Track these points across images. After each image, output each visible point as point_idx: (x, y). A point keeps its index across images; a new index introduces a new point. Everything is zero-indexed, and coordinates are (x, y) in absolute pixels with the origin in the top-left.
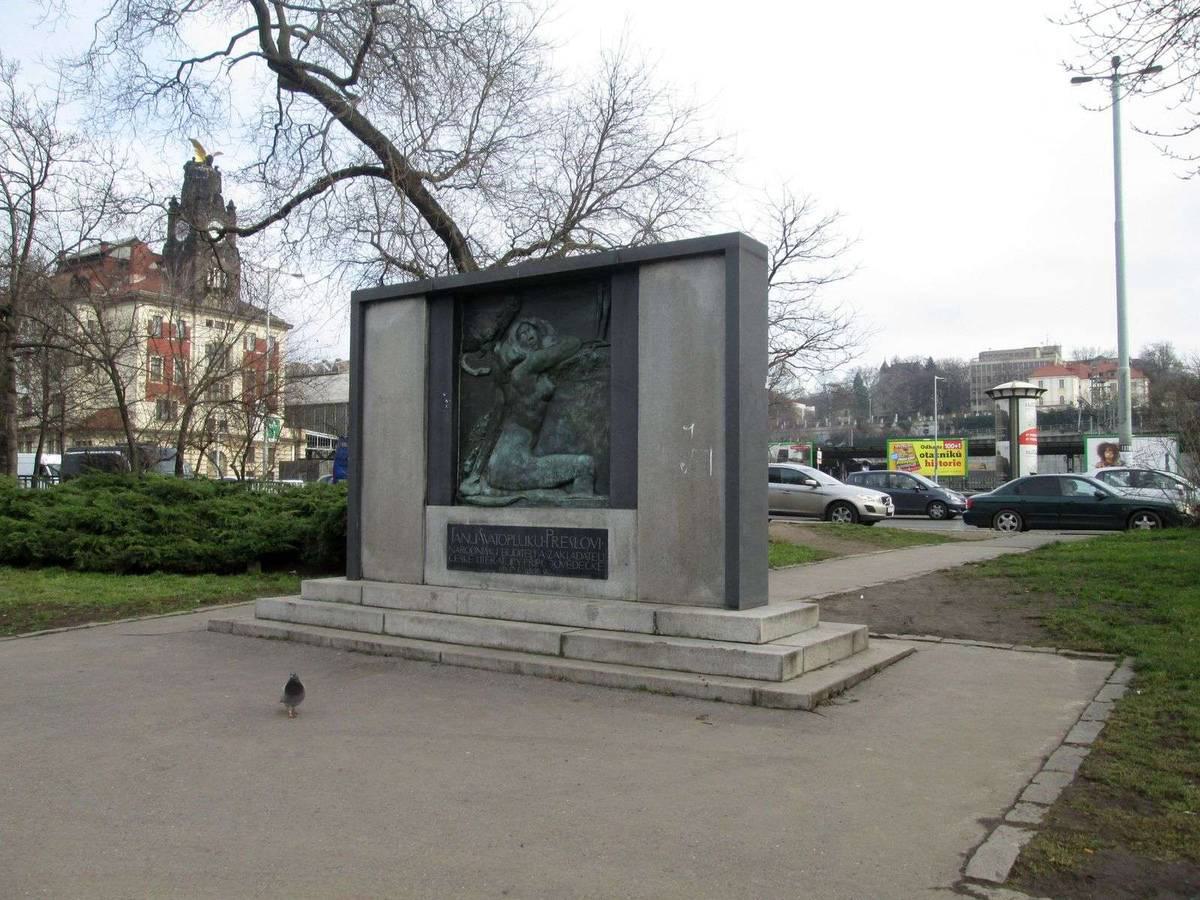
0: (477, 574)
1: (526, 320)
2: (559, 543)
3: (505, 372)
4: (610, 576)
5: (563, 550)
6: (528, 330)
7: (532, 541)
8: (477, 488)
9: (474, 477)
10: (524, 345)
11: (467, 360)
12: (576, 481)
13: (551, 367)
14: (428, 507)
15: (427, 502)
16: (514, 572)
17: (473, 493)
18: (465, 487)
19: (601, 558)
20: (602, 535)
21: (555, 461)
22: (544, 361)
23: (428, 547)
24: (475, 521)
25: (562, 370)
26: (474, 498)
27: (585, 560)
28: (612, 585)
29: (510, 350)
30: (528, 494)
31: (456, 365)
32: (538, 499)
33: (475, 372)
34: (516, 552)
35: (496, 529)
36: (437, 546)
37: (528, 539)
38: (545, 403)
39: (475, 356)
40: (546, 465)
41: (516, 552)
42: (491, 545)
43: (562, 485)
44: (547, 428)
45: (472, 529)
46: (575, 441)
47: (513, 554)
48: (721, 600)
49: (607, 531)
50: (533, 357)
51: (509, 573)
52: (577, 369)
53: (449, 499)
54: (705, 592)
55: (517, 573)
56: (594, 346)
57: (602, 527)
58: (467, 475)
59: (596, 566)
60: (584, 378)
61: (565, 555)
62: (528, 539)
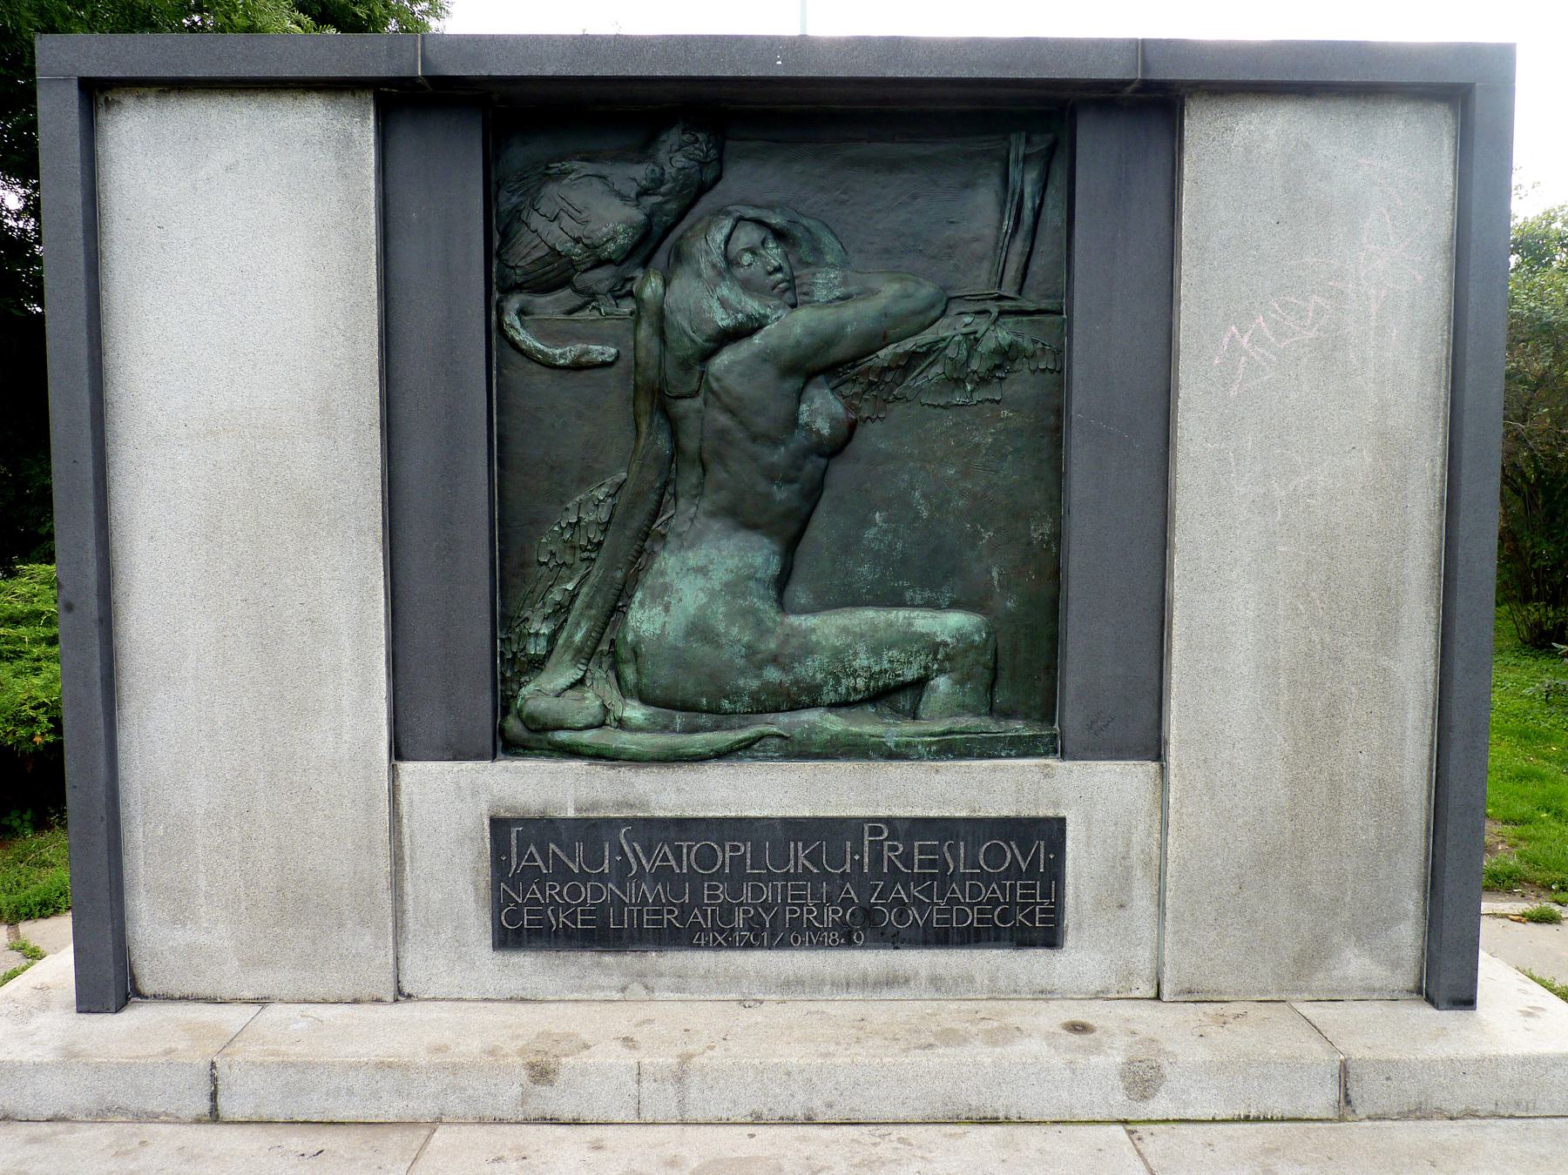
0: (608, 959)
1: (751, 213)
2: (907, 859)
3: (685, 365)
4: (1070, 939)
5: (921, 878)
6: (763, 243)
7: (814, 858)
8: (588, 704)
9: (560, 675)
10: (747, 286)
11: (522, 312)
12: (942, 683)
13: (853, 360)
14: (406, 767)
15: (398, 752)
16: (748, 946)
17: (581, 720)
20: (1051, 832)
22: (829, 341)
23: (408, 887)
24: (595, 806)
25: (889, 369)
26: (587, 737)
27: (994, 902)
28: (1078, 959)
29: (699, 297)
30: (781, 722)
31: (496, 333)
33: (565, 353)
34: (757, 891)
35: (683, 826)
36: (454, 880)
37: (799, 856)
38: (823, 462)
39: (548, 306)
41: (757, 891)
42: (663, 874)
44: (821, 530)
46: (927, 574)
47: (747, 890)
48: (1406, 977)
49: (1063, 820)
50: (790, 327)
51: (731, 946)
52: (937, 369)
54: (1355, 964)
55: (761, 947)
56: (994, 308)
57: (1050, 813)
58: (537, 665)
59: (1030, 916)
60: (958, 399)
61: (928, 892)
62: (799, 856)
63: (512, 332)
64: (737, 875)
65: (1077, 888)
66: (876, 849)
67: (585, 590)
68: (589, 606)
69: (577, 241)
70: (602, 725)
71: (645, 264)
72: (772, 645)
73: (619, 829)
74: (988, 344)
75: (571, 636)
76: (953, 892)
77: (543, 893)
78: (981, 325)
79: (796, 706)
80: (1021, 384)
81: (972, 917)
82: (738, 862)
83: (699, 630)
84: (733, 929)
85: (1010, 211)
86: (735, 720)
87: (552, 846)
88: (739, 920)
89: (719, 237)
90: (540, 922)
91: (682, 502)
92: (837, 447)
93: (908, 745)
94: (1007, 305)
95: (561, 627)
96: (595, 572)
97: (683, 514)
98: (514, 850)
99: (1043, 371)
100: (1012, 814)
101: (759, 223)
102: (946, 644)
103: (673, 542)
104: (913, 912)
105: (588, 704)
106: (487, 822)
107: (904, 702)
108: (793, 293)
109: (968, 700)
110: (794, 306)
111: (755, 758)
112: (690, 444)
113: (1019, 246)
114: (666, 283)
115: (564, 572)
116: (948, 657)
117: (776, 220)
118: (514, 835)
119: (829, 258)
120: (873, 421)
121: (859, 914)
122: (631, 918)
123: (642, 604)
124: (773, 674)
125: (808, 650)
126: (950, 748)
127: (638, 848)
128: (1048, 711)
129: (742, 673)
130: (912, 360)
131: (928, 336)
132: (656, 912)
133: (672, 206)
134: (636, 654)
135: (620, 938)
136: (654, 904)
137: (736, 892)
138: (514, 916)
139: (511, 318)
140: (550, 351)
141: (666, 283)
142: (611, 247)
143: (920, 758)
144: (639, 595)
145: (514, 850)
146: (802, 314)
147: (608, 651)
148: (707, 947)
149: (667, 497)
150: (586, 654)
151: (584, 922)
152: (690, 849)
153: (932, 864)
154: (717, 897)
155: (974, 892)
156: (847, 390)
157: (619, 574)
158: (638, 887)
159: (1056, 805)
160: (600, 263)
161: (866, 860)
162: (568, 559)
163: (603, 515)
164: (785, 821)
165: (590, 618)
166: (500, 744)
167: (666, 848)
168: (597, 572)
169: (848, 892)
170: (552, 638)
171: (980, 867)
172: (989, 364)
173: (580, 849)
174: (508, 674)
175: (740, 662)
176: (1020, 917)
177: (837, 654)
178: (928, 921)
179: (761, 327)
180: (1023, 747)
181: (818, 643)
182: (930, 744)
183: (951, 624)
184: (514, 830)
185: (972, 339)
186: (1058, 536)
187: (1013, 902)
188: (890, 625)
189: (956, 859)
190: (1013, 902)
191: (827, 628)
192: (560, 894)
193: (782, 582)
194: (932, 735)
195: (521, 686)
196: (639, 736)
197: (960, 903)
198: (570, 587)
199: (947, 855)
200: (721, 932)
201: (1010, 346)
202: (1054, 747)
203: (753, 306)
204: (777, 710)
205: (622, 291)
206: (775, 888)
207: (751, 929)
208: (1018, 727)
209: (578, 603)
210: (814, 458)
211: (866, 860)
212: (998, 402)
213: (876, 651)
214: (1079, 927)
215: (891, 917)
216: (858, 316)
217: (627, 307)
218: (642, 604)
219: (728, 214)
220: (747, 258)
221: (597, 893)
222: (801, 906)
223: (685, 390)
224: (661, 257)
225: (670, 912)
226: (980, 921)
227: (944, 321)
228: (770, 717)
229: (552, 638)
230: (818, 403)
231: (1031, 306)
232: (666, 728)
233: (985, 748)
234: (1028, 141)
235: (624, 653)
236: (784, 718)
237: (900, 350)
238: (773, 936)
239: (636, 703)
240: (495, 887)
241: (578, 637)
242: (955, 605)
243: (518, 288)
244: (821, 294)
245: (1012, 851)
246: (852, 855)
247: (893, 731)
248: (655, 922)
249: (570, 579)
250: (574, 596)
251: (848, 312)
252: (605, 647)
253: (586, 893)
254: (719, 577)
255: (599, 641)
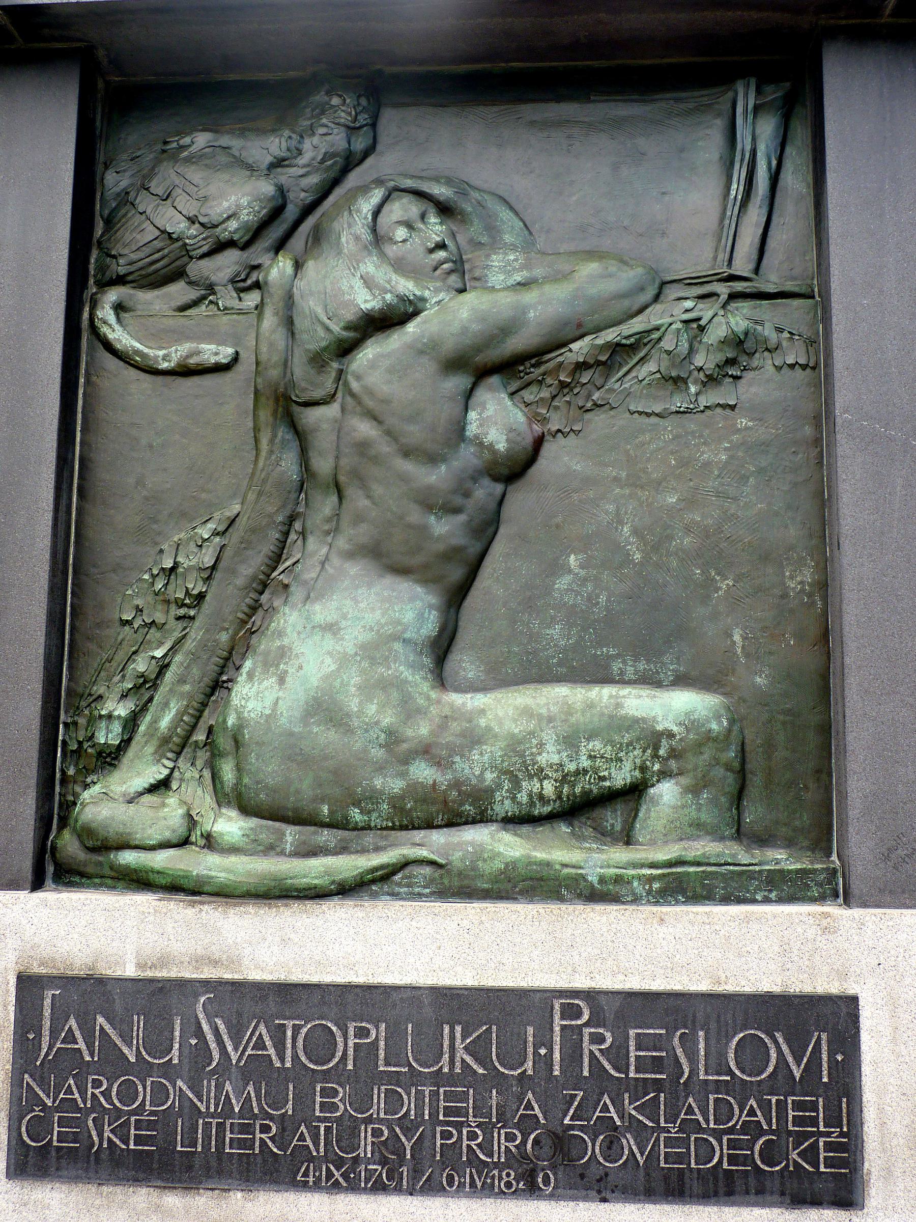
1: (409, 183)
2: (618, 1054)
3: (318, 360)
4: (876, 1193)
6: (423, 217)
7: (478, 1050)
8: (169, 815)
10: (400, 266)
11: (119, 308)
12: (666, 792)
13: (536, 355)
16: (379, 1188)
17: (154, 835)
18: (105, 803)
19: (833, 1120)
21: (569, 710)
22: (505, 330)
24: (164, 961)
25: (581, 366)
26: (160, 860)
29: (343, 279)
30: (435, 843)
32: (498, 865)
35: (287, 994)
38: (499, 488)
39: (157, 302)
40: (518, 719)
42: (256, 1069)
43: (591, 807)
45: (157, 997)
49: (854, 1000)
50: (453, 315)
51: (353, 1187)
52: (651, 366)
53: (27, 865)
55: (398, 1190)
58: (110, 758)
59: (811, 1154)
61: (650, 1110)
62: (456, 1046)
63: (105, 329)
64: (364, 1076)
65: (881, 1110)
66: (572, 1036)
67: (178, 658)
68: (182, 681)
69: (192, 220)
70: (184, 843)
71: (279, 247)
72: (423, 730)
73: (196, 996)
74: (717, 332)
75: (155, 721)
76: (690, 1111)
77: (83, 1092)
78: (706, 311)
79: (455, 820)
80: (761, 384)
81: (720, 1152)
82: (366, 1053)
83: (324, 708)
84: (356, 1160)
85: (739, 174)
86: (369, 838)
87: (100, 1020)
88: (366, 1148)
89: (366, 206)
90: (75, 1138)
91: (311, 540)
92: (514, 469)
93: (618, 880)
94: (739, 286)
95: (144, 709)
96: (193, 634)
97: (312, 553)
98: (47, 1024)
99: (792, 366)
100: (777, 989)
101: (419, 194)
102: (671, 735)
103: (297, 593)
104: (629, 1142)
105: (169, 815)
106: (13, 981)
107: (613, 818)
108: (461, 274)
109: (704, 817)
110: (462, 291)
111: (395, 895)
112: (323, 465)
113: (755, 215)
114: (298, 266)
115: (153, 633)
116: (674, 754)
117: (439, 191)
118: (48, 1002)
119: (508, 238)
120: (565, 435)
121: (547, 1142)
122: (207, 1137)
123: (250, 676)
124: (423, 772)
125: (474, 739)
126: (680, 886)
127: (222, 1027)
128: (821, 834)
129: (380, 768)
130: (620, 351)
131: (637, 325)
132: (246, 1129)
133: (314, 180)
134: (237, 743)
135: (190, 1168)
136: (241, 1116)
137: (363, 1102)
138: (39, 1128)
139: (106, 312)
140: (151, 352)
141: (298, 266)
142: (233, 225)
143: (636, 900)
144: (248, 664)
145: (47, 1024)
146: (469, 297)
147: (202, 739)
148: (317, 1187)
149: (293, 536)
150: (178, 745)
151: (139, 1140)
152: (298, 1030)
153: (657, 1064)
154: (334, 1107)
155: (723, 1112)
156: (529, 395)
157: (224, 637)
158: (219, 1087)
159: (843, 975)
160: (221, 246)
161: (557, 1056)
162: (159, 617)
163: (208, 560)
164: (435, 990)
165: (182, 695)
166: (50, 869)
167: (262, 1029)
168: (196, 633)
169: (529, 1106)
170: (131, 723)
171: (730, 1072)
172: (720, 357)
173: (139, 1023)
174: (71, 772)
175: (377, 753)
176: (794, 1155)
177: (515, 745)
178: (652, 1157)
179: (416, 313)
180: (788, 888)
181: (489, 729)
182: (651, 879)
183: (676, 707)
184: (49, 994)
185: (695, 326)
186: (824, 586)
187: (781, 1131)
188: (590, 706)
189: (692, 1058)
190: (781, 1131)
191: (504, 711)
192: (106, 1094)
193: (441, 649)
194: (653, 866)
195: (86, 786)
196: (233, 860)
197: (700, 1130)
198: (158, 653)
199: (679, 1051)
200: (339, 1165)
201: (746, 334)
202: (836, 889)
203: (407, 286)
204: (430, 825)
205: (248, 282)
206: (420, 1095)
207: (384, 1162)
208: (778, 858)
209: (169, 676)
210: (486, 481)
211: (557, 1056)
212: (733, 408)
213: (570, 742)
214: (888, 1172)
215: (595, 1148)
216: (543, 308)
217: (252, 299)
218: (250, 676)
219: (379, 182)
220: (401, 233)
221: (160, 1094)
222: (459, 1126)
223: (318, 394)
224: (298, 242)
225: (265, 1129)
226: (732, 1160)
227: (658, 307)
228: (419, 835)
229: (131, 723)
230: (491, 409)
231: (771, 288)
232: (270, 849)
233: (731, 888)
234: (759, 92)
235: (224, 742)
236: (438, 837)
237: (600, 341)
238: (416, 1172)
239: (233, 813)
240: (16, 1081)
241: (165, 722)
242: (682, 681)
243: (120, 280)
244: (496, 279)
245: (778, 1048)
246: (536, 1047)
247: (595, 859)
248: (242, 1143)
249: (160, 644)
250: (163, 668)
251: (529, 297)
252: (200, 736)
253: (144, 1093)
254: (354, 636)
255: (194, 727)
